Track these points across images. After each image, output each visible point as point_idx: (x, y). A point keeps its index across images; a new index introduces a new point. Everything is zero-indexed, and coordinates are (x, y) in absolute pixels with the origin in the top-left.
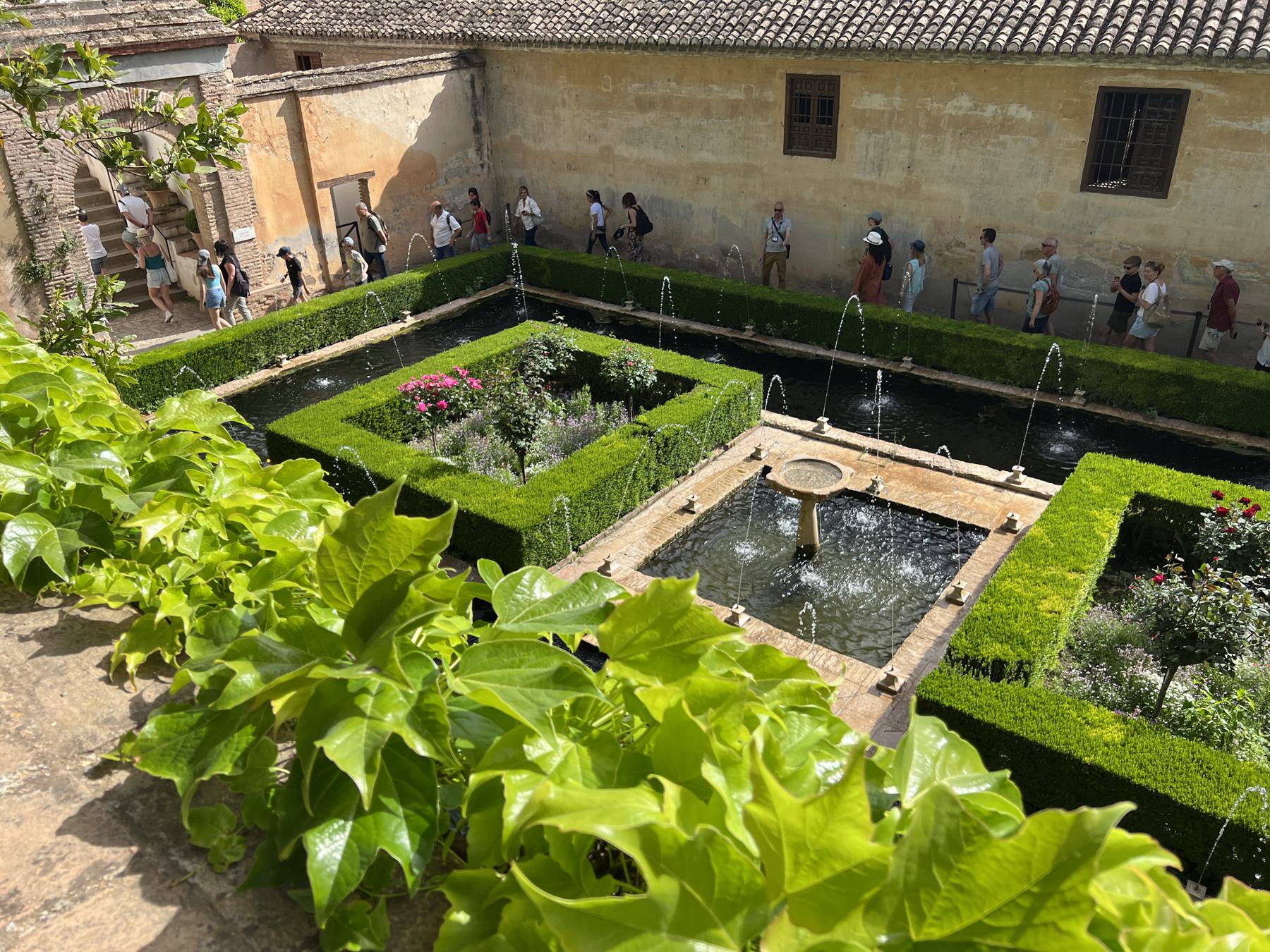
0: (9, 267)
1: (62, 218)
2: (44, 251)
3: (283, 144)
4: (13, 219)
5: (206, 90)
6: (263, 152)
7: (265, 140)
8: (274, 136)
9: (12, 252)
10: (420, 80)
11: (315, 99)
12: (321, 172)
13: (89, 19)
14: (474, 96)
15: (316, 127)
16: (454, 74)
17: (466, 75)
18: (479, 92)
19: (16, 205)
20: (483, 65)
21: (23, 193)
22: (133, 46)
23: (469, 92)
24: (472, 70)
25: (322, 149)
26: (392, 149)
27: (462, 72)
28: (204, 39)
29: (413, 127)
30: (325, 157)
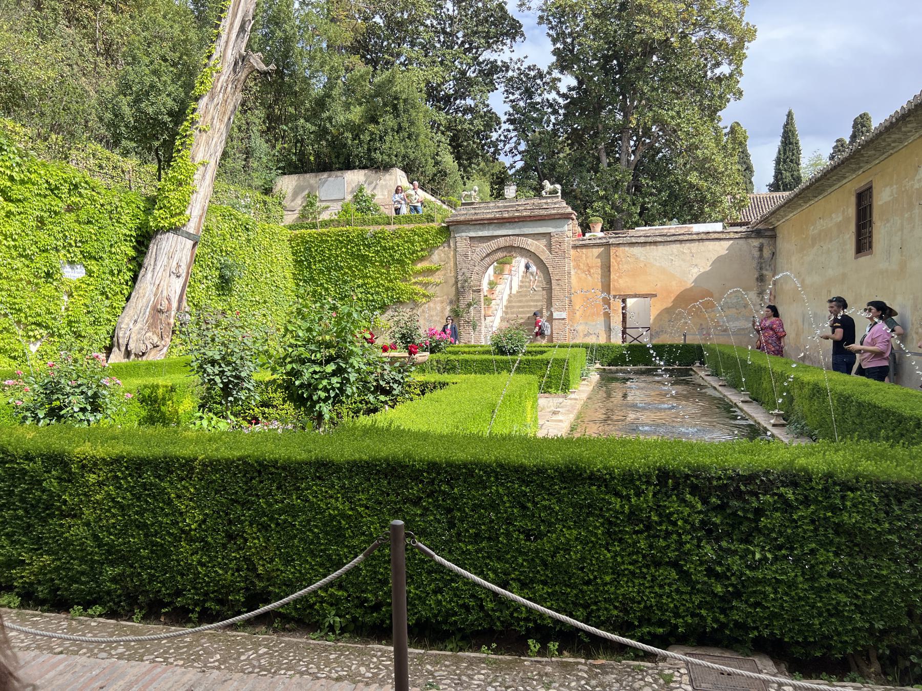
0: (448, 308)
1: (474, 291)
2: (462, 305)
3: (597, 273)
4: (454, 288)
5: (553, 240)
6: (584, 275)
7: (586, 269)
8: (592, 267)
9: (451, 302)
10: (707, 243)
11: (621, 249)
12: (616, 289)
13: (505, 207)
14: (761, 257)
15: (618, 264)
16: (742, 242)
17: (756, 243)
18: (767, 253)
19: (456, 282)
20: (774, 237)
21: (460, 278)
22: (518, 217)
23: (756, 254)
24: (761, 240)
25: (620, 277)
26: (674, 283)
27: (750, 241)
28: (555, 215)
29: (695, 272)
30: (621, 281)
